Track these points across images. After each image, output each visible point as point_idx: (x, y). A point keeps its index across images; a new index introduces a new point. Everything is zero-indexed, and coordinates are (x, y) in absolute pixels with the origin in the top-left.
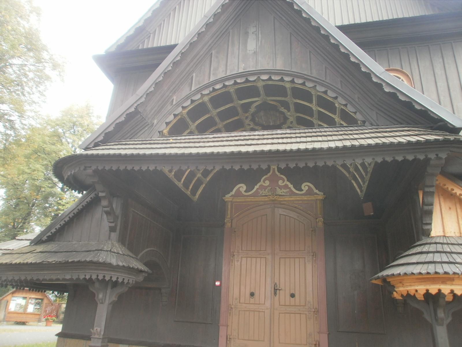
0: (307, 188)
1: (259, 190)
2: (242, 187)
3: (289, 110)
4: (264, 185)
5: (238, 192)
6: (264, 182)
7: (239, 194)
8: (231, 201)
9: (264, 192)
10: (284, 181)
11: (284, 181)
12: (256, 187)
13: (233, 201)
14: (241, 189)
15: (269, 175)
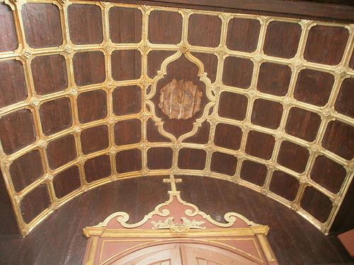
0: (235, 219)
1: (152, 222)
2: (123, 217)
3: (213, 81)
4: (161, 214)
5: (115, 221)
6: (160, 210)
7: (116, 225)
8: (100, 237)
9: (162, 224)
10: (194, 210)
11: (194, 210)
12: (146, 218)
13: (103, 236)
14: (119, 219)
15: (167, 203)
